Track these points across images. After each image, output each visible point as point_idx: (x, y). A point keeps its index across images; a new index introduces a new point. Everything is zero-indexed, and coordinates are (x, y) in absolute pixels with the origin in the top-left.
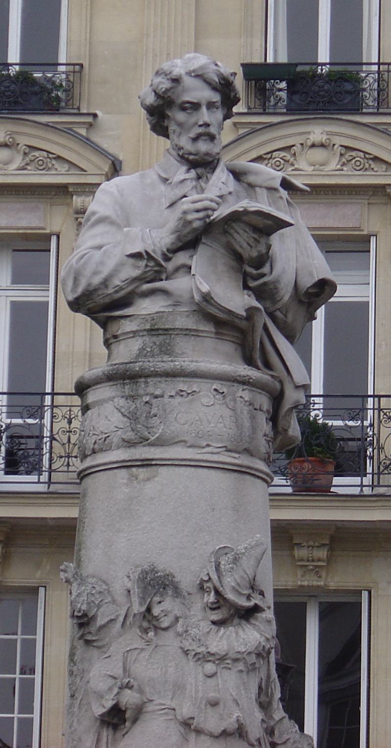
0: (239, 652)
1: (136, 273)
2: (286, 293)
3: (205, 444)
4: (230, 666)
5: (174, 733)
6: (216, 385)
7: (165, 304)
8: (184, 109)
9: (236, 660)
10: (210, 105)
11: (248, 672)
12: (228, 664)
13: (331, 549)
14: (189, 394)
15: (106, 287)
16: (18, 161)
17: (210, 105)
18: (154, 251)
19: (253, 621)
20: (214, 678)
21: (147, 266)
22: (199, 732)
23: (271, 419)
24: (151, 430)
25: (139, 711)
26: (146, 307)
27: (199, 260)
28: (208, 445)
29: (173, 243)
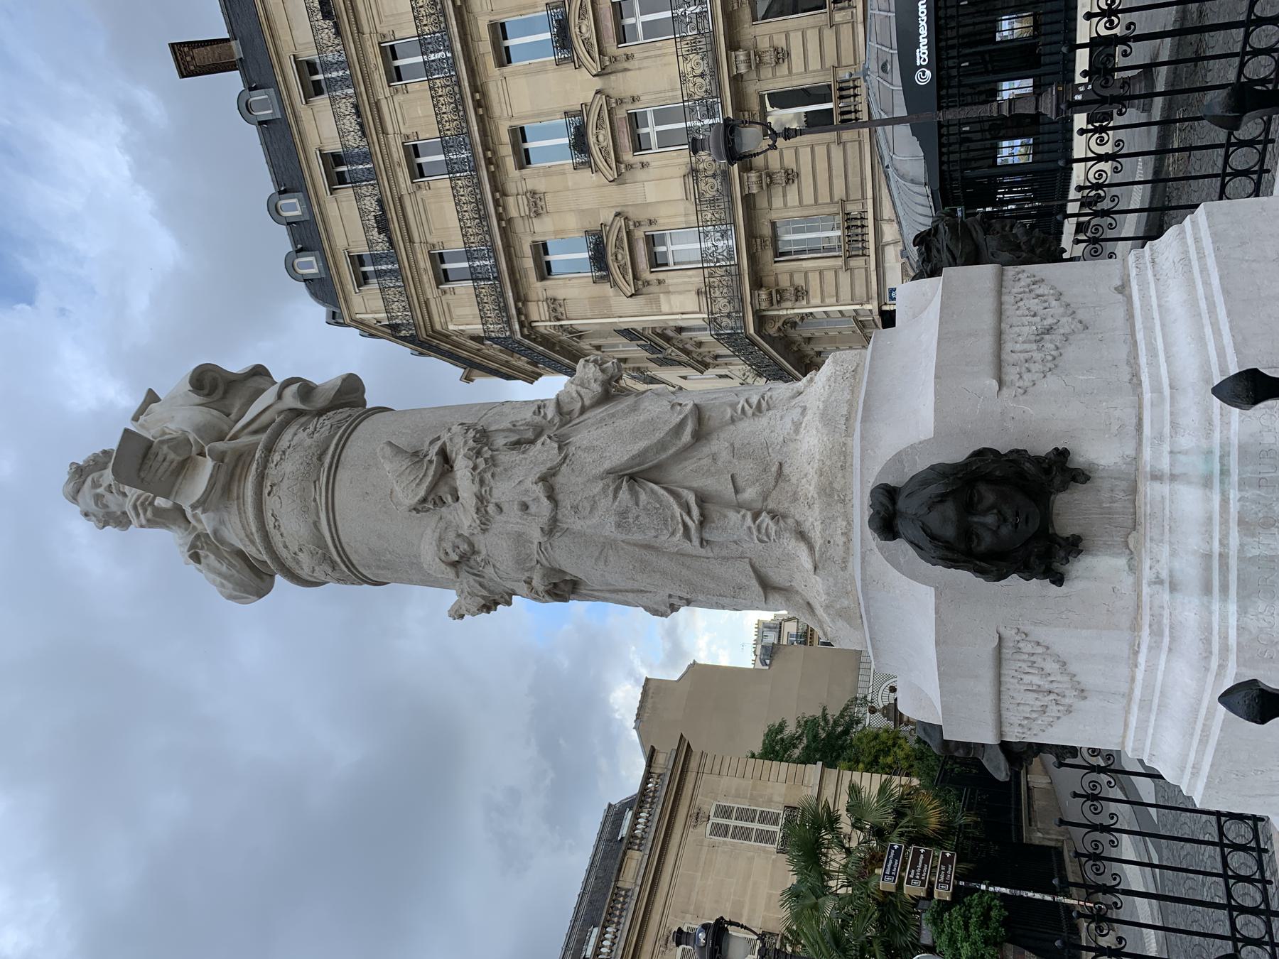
0: (473, 480)
1: (212, 557)
3: (313, 503)
4: (488, 489)
5: (560, 542)
6: (266, 491)
7: (226, 530)
8: (106, 506)
9: (482, 482)
11: (495, 465)
12: (486, 491)
13: (745, 110)
14: (276, 520)
15: (232, 576)
16: (620, 251)
18: (186, 544)
19: (454, 455)
20: (502, 506)
21: (202, 548)
22: (554, 521)
23: (266, 450)
24: (314, 552)
28: (315, 500)
29: (180, 527)
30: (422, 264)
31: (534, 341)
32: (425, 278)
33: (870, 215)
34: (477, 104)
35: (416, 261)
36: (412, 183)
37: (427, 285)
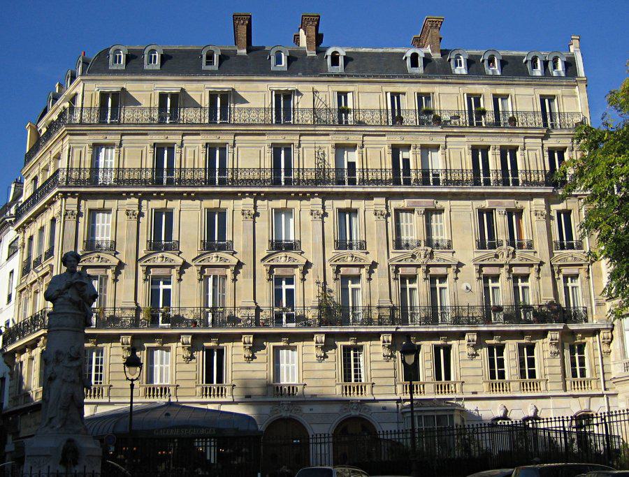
2: (88, 297)
10: (74, 261)
17: (74, 261)
25: (55, 378)
26: (60, 300)
27: (69, 291)
30: (109, 137)
31: (54, 196)
32: (100, 137)
33: (100, 400)
34: (189, 193)
35: (111, 134)
36: (155, 144)
37: (96, 137)
